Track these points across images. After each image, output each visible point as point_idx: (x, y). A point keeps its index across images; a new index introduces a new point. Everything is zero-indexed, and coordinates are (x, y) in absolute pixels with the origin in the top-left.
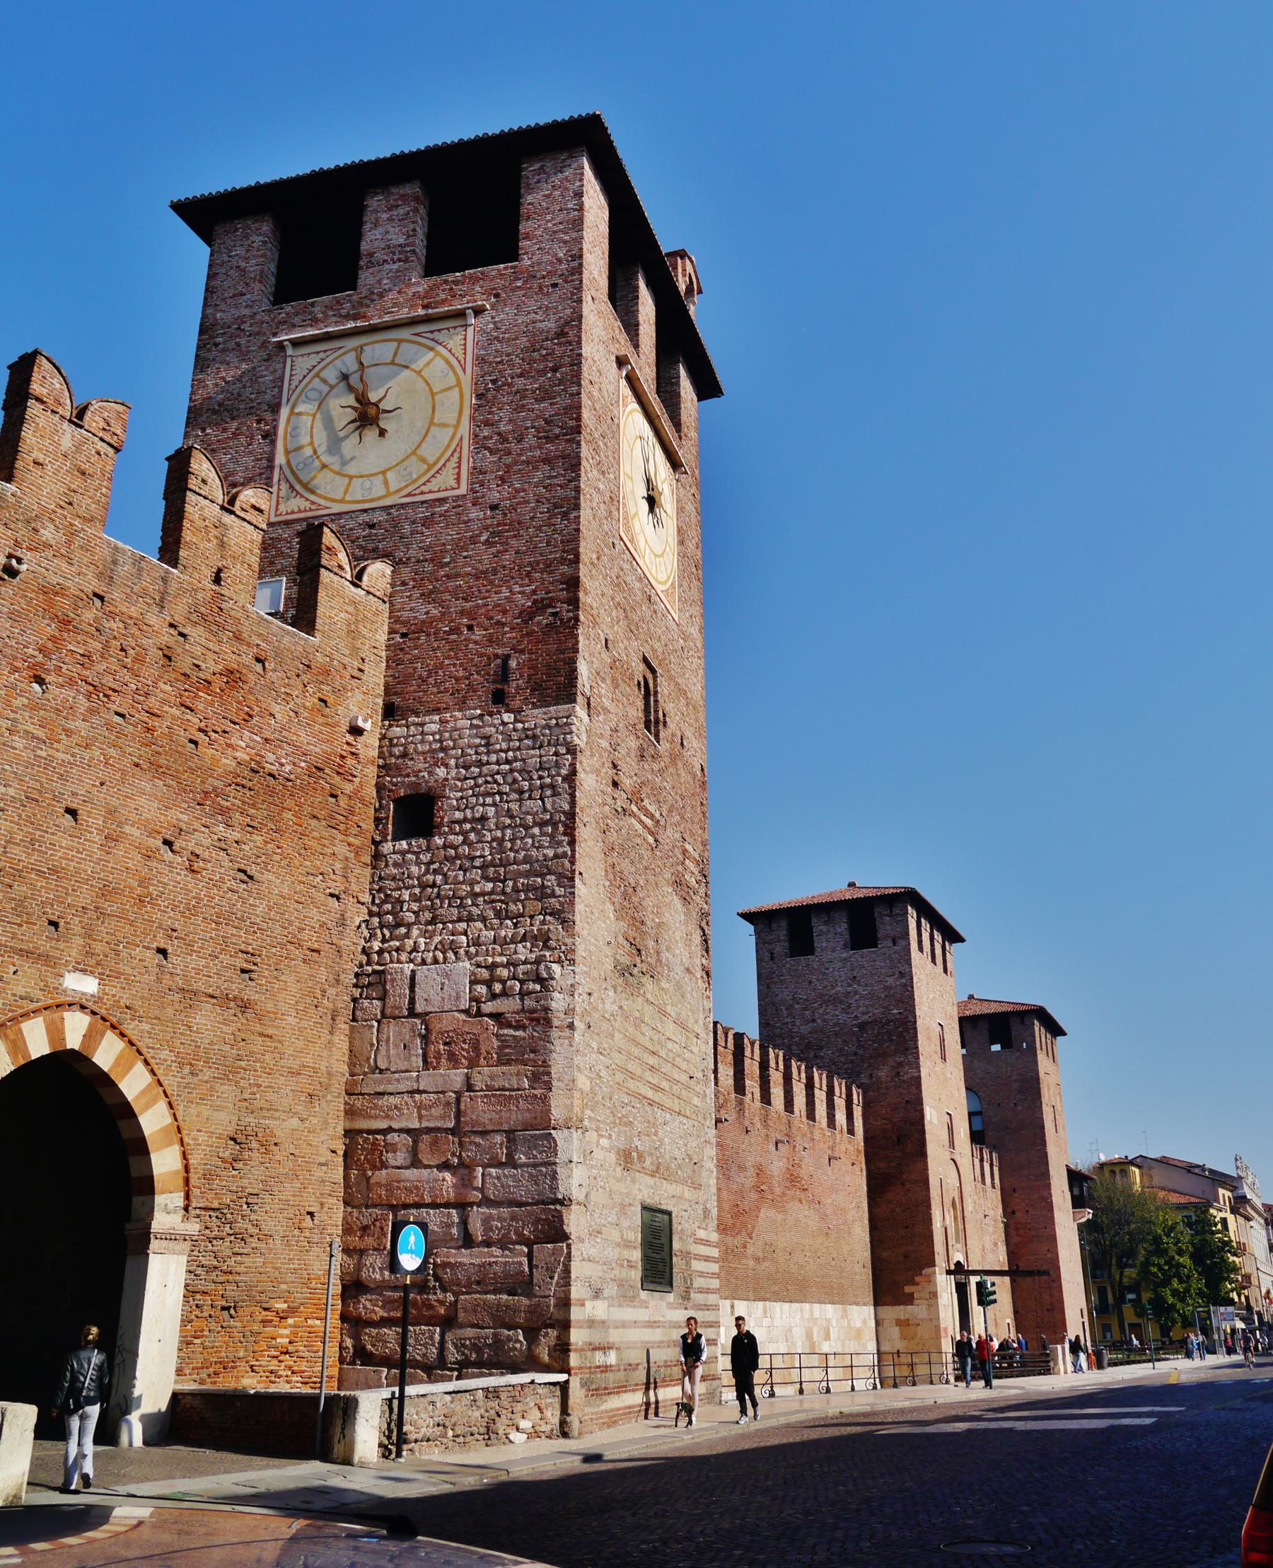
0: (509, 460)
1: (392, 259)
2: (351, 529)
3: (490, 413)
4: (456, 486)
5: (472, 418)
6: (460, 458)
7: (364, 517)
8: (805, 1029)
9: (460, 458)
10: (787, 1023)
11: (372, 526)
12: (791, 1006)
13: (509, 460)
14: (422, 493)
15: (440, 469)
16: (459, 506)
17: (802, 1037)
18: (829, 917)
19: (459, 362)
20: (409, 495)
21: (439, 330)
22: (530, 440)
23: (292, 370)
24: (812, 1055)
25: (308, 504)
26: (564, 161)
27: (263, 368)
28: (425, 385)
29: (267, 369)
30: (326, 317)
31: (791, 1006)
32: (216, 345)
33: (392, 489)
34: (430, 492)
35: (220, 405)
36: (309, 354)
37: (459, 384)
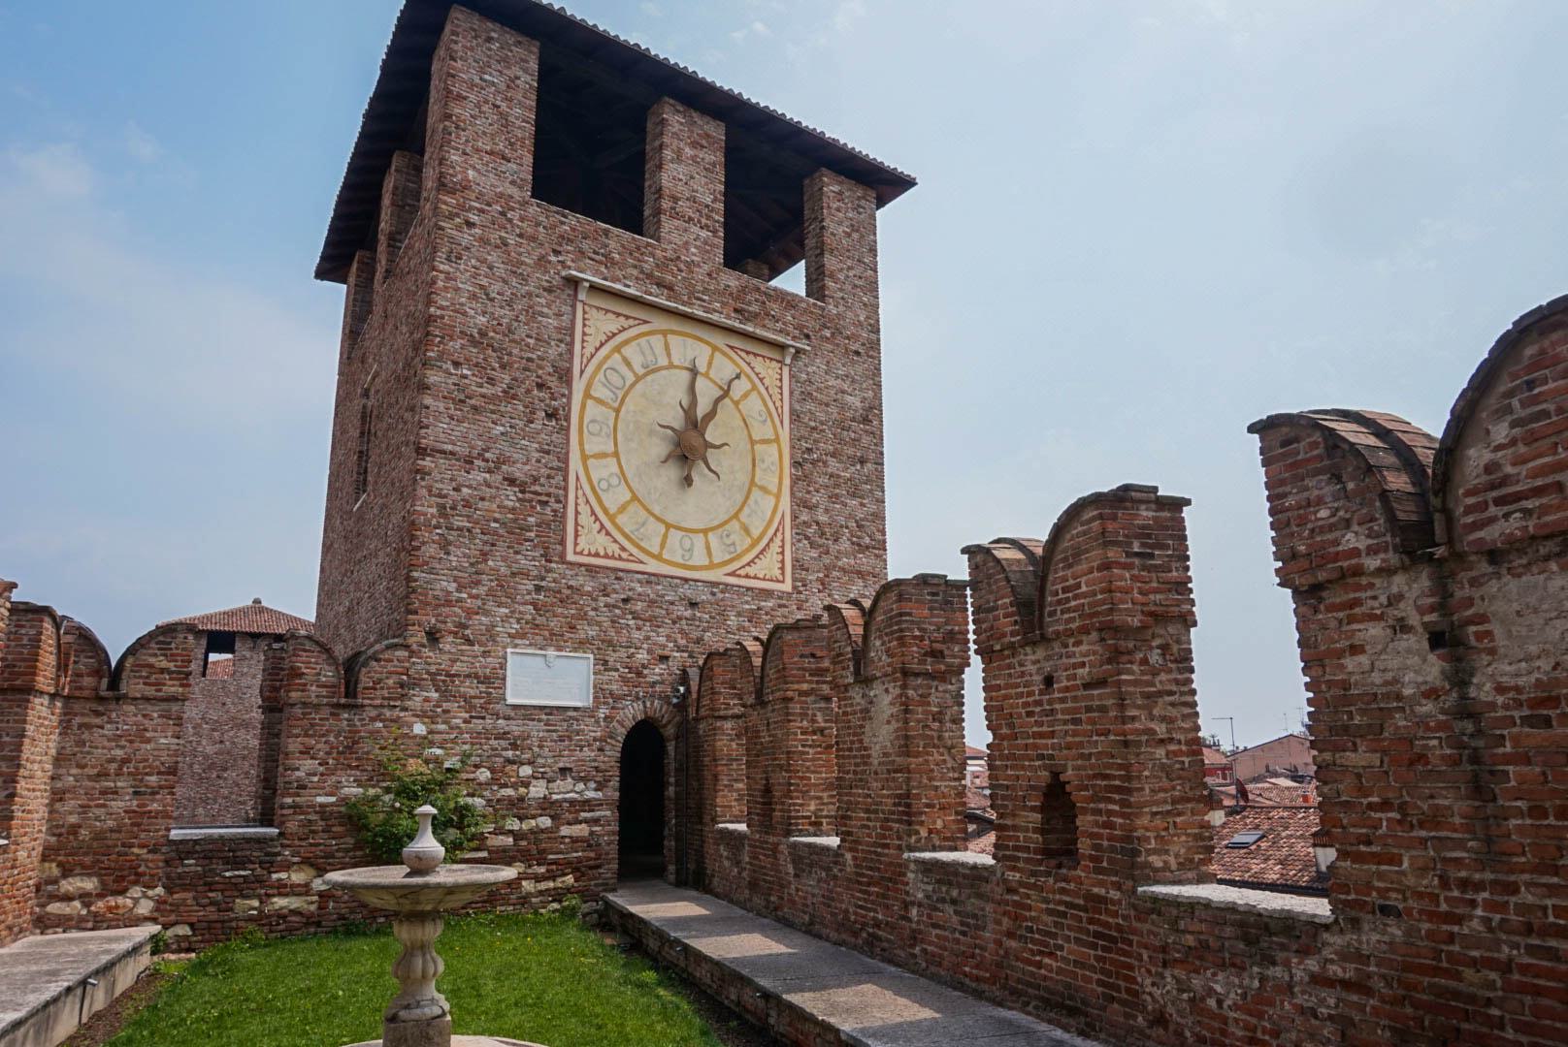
0: (827, 560)
1: (699, 221)
2: (672, 603)
3: (809, 492)
4: (780, 578)
5: (792, 494)
6: (783, 541)
7: (686, 591)
8: (210, 750)
9: (783, 541)
10: (191, 742)
11: (693, 605)
12: (200, 725)
13: (827, 560)
14: (747, 576)
15: (764, 550)
16: (785, 606)
17: (206, 757)
18: (255, 643)
19: (777, 409)
20: (733, 574)
21: (756, 355)
22: (845, 545)
23: (584, 325)
24: (214, 776)
25: (616, 547)
26: (859, 198)
27: (543, 301)
28: (742, 424)
29: (549, 306)
30: (622, 266)
31: (200, 725)
32: (470, 224)
33: (716, 561)
34: (755, 577)
35: (483, 334)
36: (607, 311)
37: (777, 440)
